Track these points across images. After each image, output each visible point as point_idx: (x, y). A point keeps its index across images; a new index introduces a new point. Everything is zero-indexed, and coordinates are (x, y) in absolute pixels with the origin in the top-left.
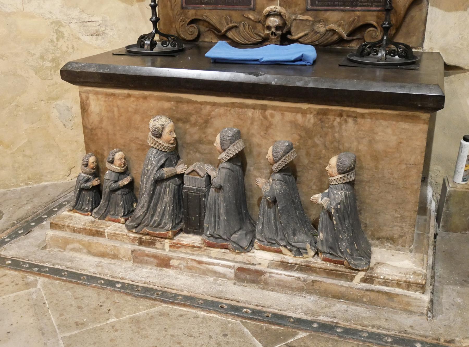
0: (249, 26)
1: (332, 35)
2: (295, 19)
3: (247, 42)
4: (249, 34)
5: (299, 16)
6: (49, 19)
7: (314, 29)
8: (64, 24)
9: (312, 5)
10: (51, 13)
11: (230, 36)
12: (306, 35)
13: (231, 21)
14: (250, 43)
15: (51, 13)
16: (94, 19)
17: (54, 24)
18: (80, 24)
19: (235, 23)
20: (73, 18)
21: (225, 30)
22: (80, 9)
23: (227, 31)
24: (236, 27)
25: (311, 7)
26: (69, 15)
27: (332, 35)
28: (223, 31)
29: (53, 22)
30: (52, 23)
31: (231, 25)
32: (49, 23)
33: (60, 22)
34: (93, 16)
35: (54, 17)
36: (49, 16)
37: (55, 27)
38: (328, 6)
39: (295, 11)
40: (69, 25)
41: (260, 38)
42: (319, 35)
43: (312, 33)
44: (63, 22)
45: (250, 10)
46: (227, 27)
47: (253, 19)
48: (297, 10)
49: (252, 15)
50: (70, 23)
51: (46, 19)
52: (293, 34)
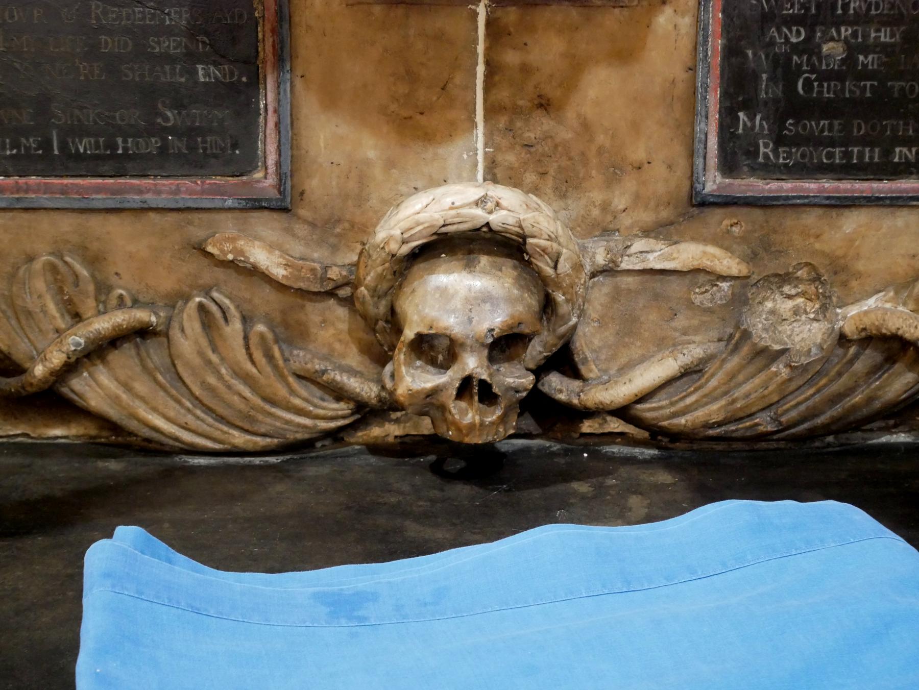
0: (246, 320)
1: (875, 370)
2: (609, 271)
3: (239, 439)
4: (247, 379)
5: (638, 245)
7: (746, 335)
9: (728, 166)
11: (95, 401)
12: (691, 373)
13: (103, 289)
14: (261, 442)
19: (136, 303)
21: (57, 359)
23: (71, 368)
24: (143, 332)
25: (719, 179)
27: (875, 370)
28: (39, 370)
31: (103, 325)
38: (847, 170)
39: (605, 207)
41: (343, 408)
42: (780, 369)
43: (734, 362)
45: (256, 205)
46: (76, 340)
47: (279, 273)
48: (620, 202)
49: (271, 247)
52: (591, 371)
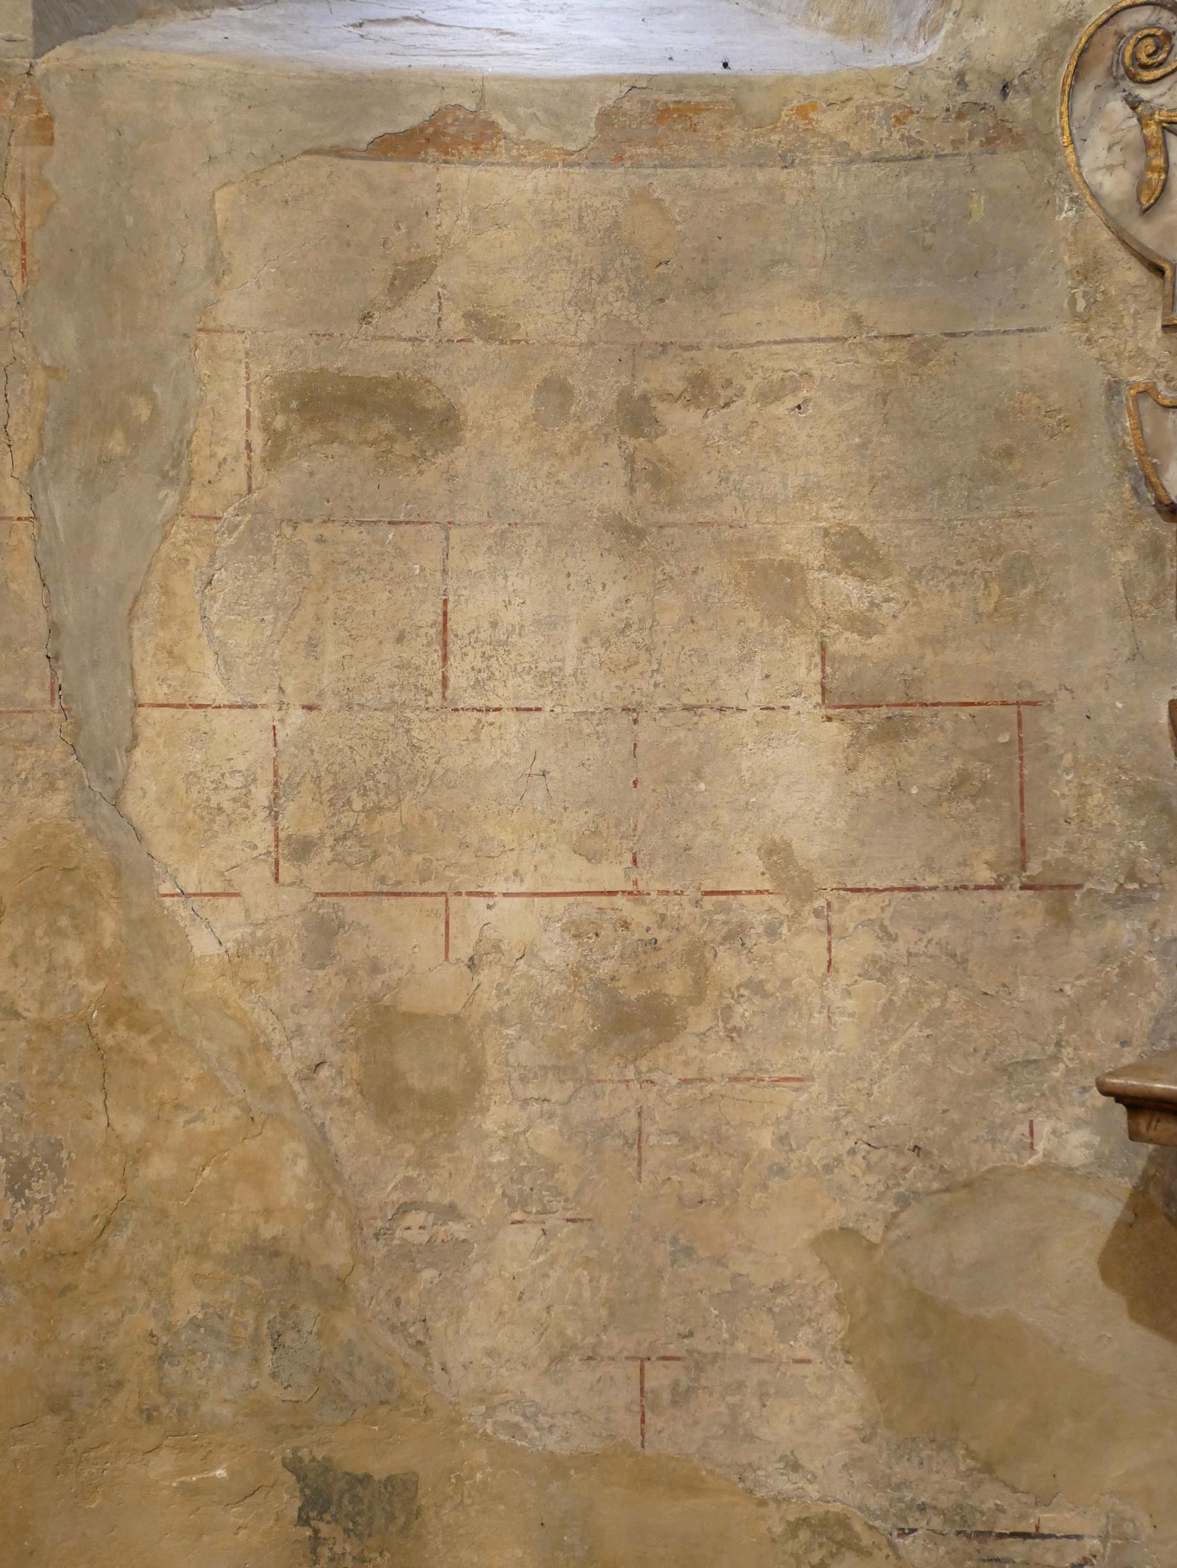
6: (781, 1500)
8: (866, 1540)
10: (796, 1467)
15: (796, 1467)
16: (1049, 1520)
17: (804, 1535)
18: (958, 1543)
20: (922, 1508)
22: (970, 1454)
26: (898, 1487)
29: (804, 1522)
30: (794, 1528)
32: (779, 1529)
33: (843, 1522)
34: (1043, 1501)
35: (813, 1491)
36: (784, 1484)
37: (808, 1550)
40: (892, 1545)
44: (858, 1527)
50: (903, 1533)
51: (762, 1503)
